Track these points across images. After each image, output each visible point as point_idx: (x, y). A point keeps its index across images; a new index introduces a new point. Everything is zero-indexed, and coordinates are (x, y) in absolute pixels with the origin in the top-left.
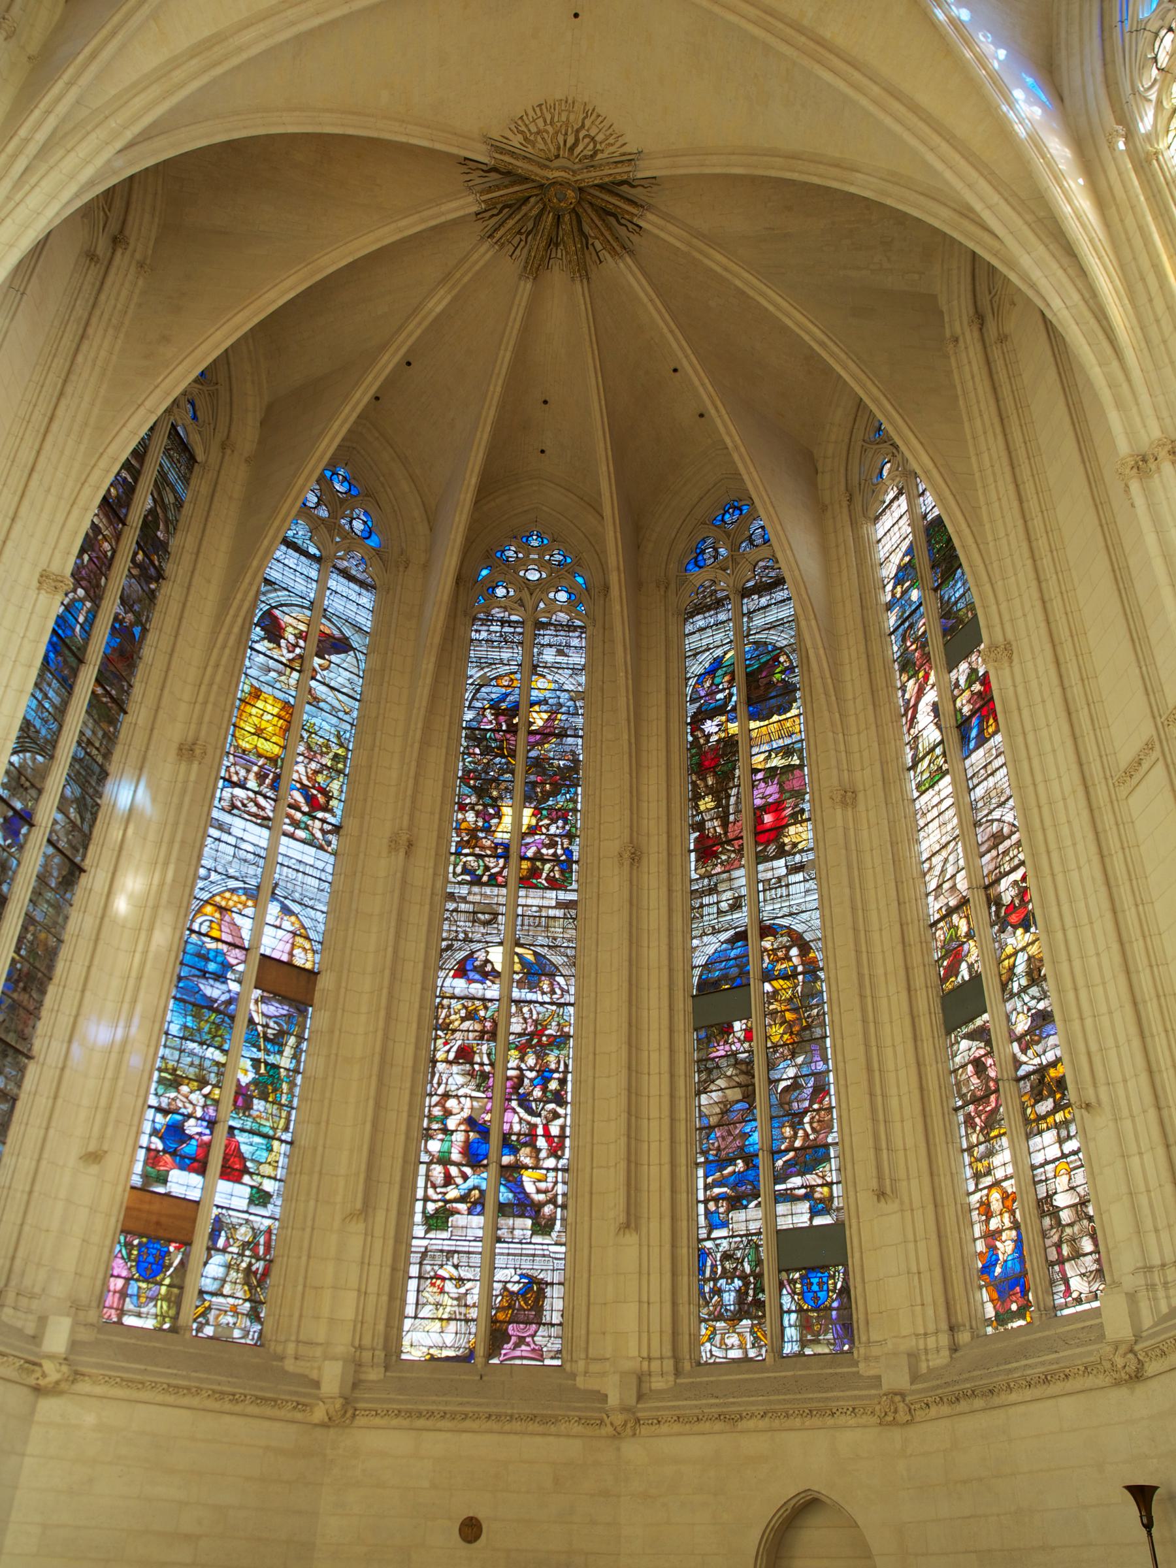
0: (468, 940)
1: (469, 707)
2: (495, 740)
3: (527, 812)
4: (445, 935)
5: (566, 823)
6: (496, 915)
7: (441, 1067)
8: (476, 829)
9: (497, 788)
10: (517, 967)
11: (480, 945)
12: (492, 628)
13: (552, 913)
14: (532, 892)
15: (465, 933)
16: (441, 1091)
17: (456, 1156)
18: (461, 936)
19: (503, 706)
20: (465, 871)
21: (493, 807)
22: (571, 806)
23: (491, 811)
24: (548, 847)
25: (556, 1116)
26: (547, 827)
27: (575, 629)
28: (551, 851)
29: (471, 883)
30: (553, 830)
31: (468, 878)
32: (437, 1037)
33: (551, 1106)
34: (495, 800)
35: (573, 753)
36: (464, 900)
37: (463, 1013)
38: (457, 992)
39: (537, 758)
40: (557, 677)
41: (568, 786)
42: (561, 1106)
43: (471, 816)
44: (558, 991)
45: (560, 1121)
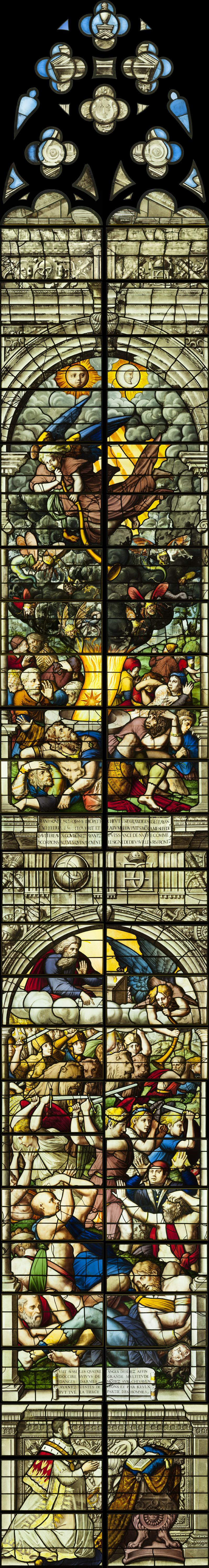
3: (115, 663)
7: (19, 1142)
16: (23, 1180)
17: (55, 1281)
20: (30, 790)
24: (155, 732)
25: (187, 1209)
31: (34, 802)
32: (11, 1093)
33: (178, 1194)
37: (47, 1051)
38: (35, 1014)
42: (192, 1194)
44: (180, 1003)
45: (192, 1218)
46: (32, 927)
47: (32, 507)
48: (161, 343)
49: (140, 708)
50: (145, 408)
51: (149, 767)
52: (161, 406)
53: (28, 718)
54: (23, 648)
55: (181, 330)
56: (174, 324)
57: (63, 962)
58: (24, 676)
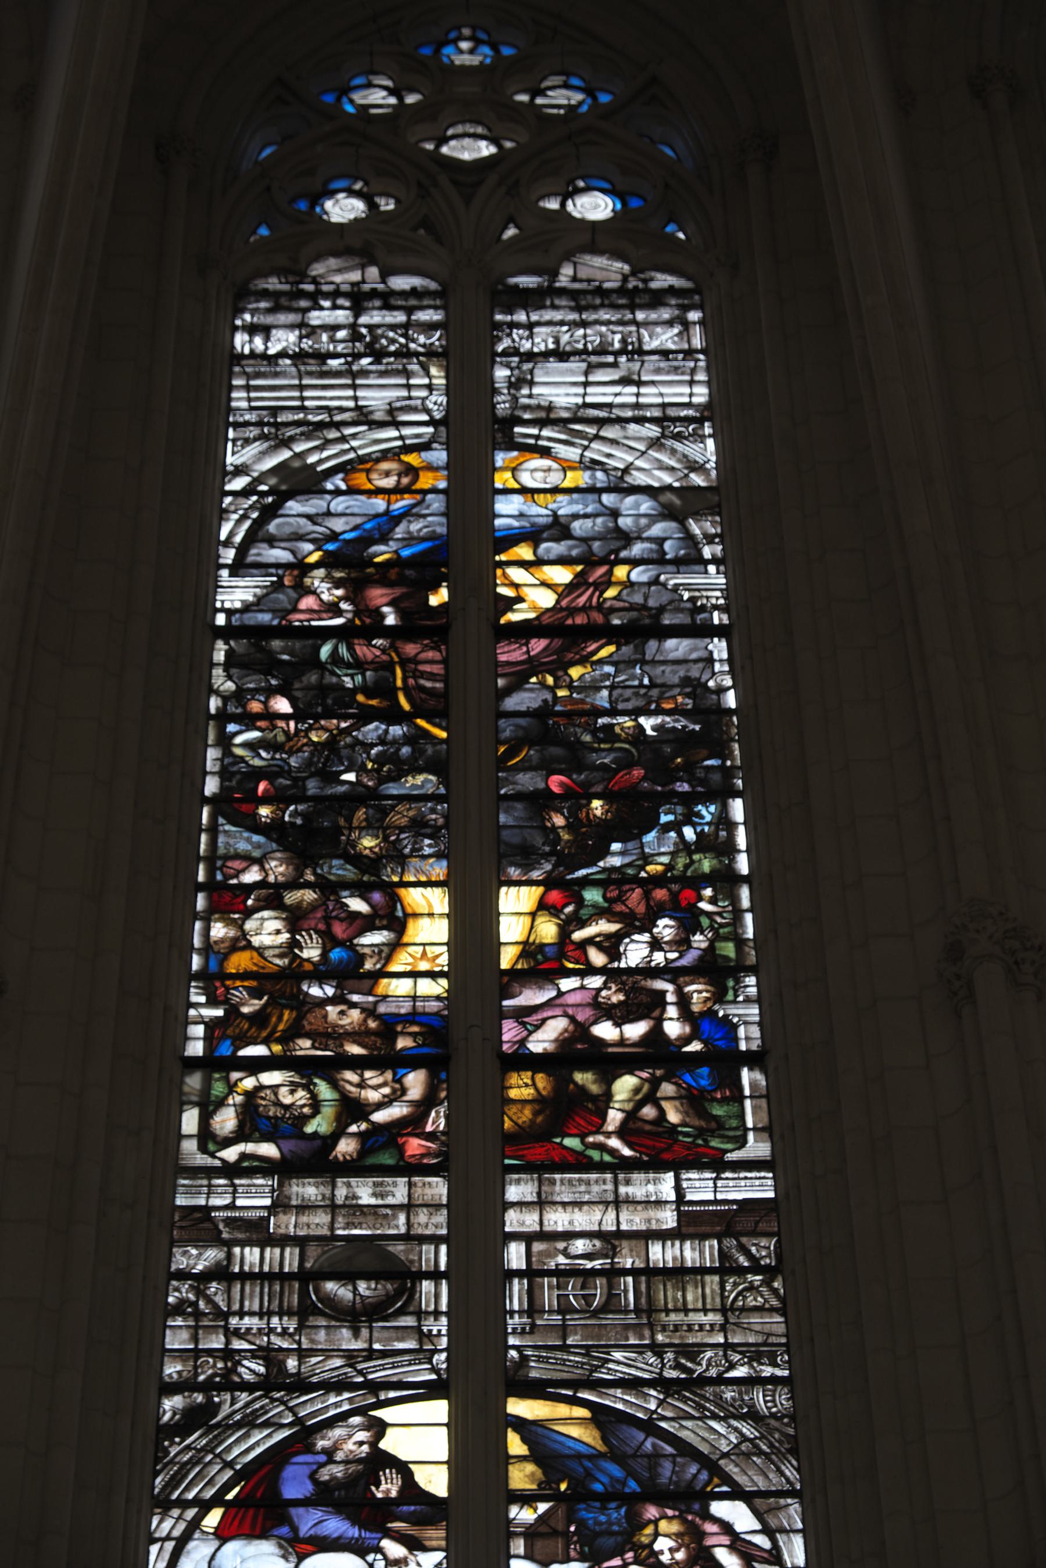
0: (276, 1381)
1: (238, 568)
2: (359, 665)
4: (172, 1369)
5: (689, 922)
6: (404, 1279)
8: (297, 972)
9: (376, 825)
10: (521, 1477)
11: (338, 1402)
12: (316, 318)
13: (658, 1254)
14: (564, 1186)
15: (268, 1355)
18: (251, 1369)
19: (382, 553)
20: (254, 1121)
21: (362, 890)
22: (706, 865)
23: (357, 905)
26: (612, 946)
27: (656, 299)
28: (636, 1030)
29: (283, 1170)
30: (635, 953)
31: (269, 1150)
34: (370, 864)
35: (695, 687)
36: (256, 1231)
39: (543, 713)
40: (597, 451)
41: (689, 800)
43: (267, 930)
46: (244, 1397)
47: (285, 657)
48: (609, 432)
49: (582, 974)
50: (576, 516)
51: (608, 1079)
52: (615, 514)
53: (256, 994)
54: (252, 876)
55: (657, 413)
56: (637, 406)
57: (337, 1471)
58: (250, 925)
